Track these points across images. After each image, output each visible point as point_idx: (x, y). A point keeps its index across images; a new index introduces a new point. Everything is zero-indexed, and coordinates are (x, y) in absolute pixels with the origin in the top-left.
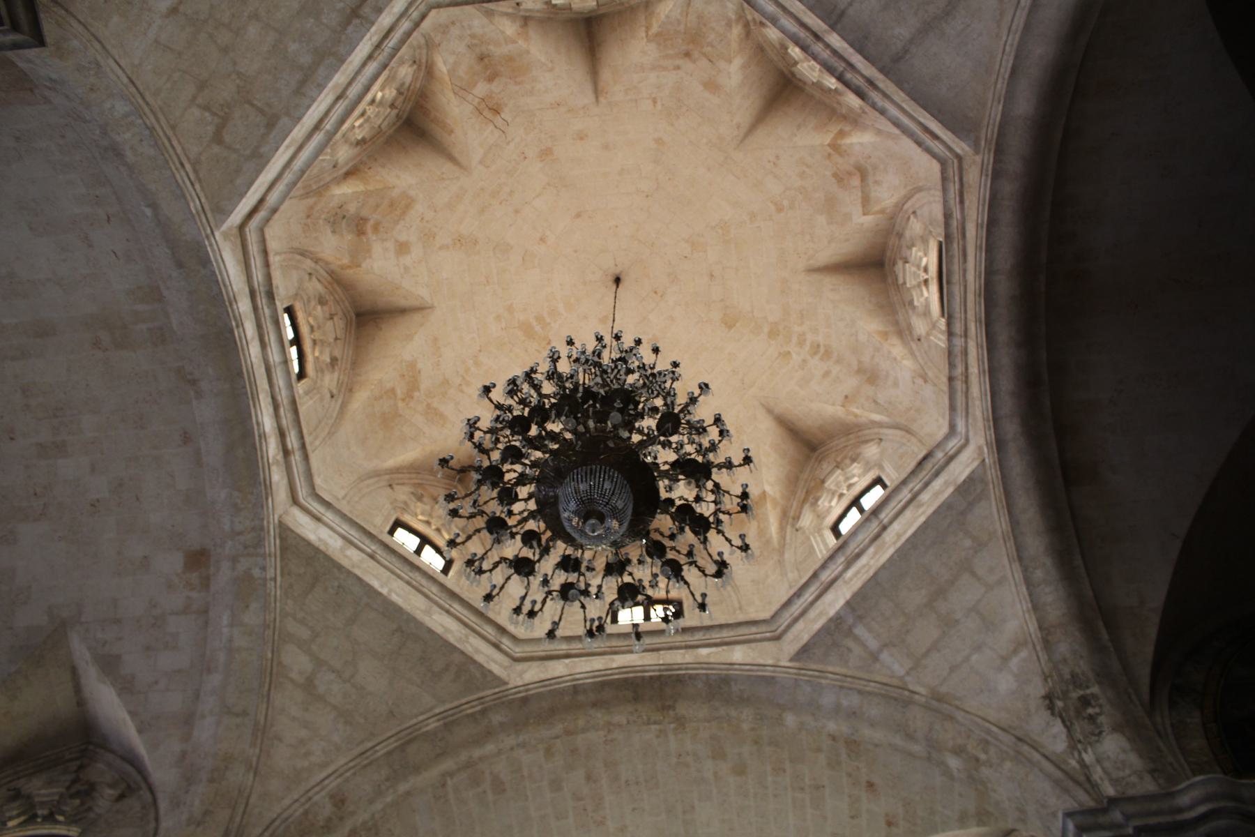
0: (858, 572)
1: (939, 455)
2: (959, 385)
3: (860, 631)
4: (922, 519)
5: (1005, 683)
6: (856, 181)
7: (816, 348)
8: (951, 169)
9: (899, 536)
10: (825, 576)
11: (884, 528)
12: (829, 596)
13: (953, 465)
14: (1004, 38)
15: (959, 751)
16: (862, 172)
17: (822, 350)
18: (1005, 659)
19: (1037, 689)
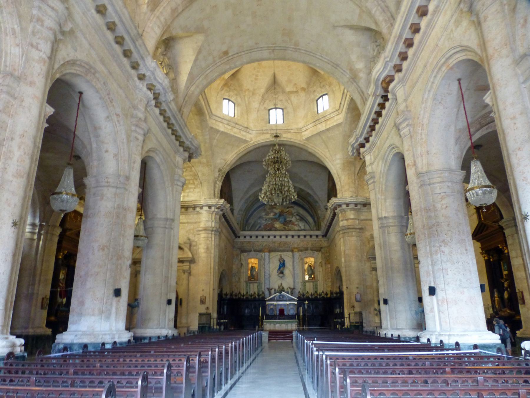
0: (227, 128)
1: (248, 130)
2: (261, 131)
3: (218, 135)
4: (239, 136)
5: (219, 161)
6: (295, 90)
7: (257, 76)
8: (299, 131)
9: (235, 133)
10: (223, 121)
11: (235, 127)
12: (221, 125)
13: (247, 134)
14: (320, 150)
15: (207, 162)
16: (297, 92)
17: (257, 78)
18: (222, 159)
19: (220, 167)
